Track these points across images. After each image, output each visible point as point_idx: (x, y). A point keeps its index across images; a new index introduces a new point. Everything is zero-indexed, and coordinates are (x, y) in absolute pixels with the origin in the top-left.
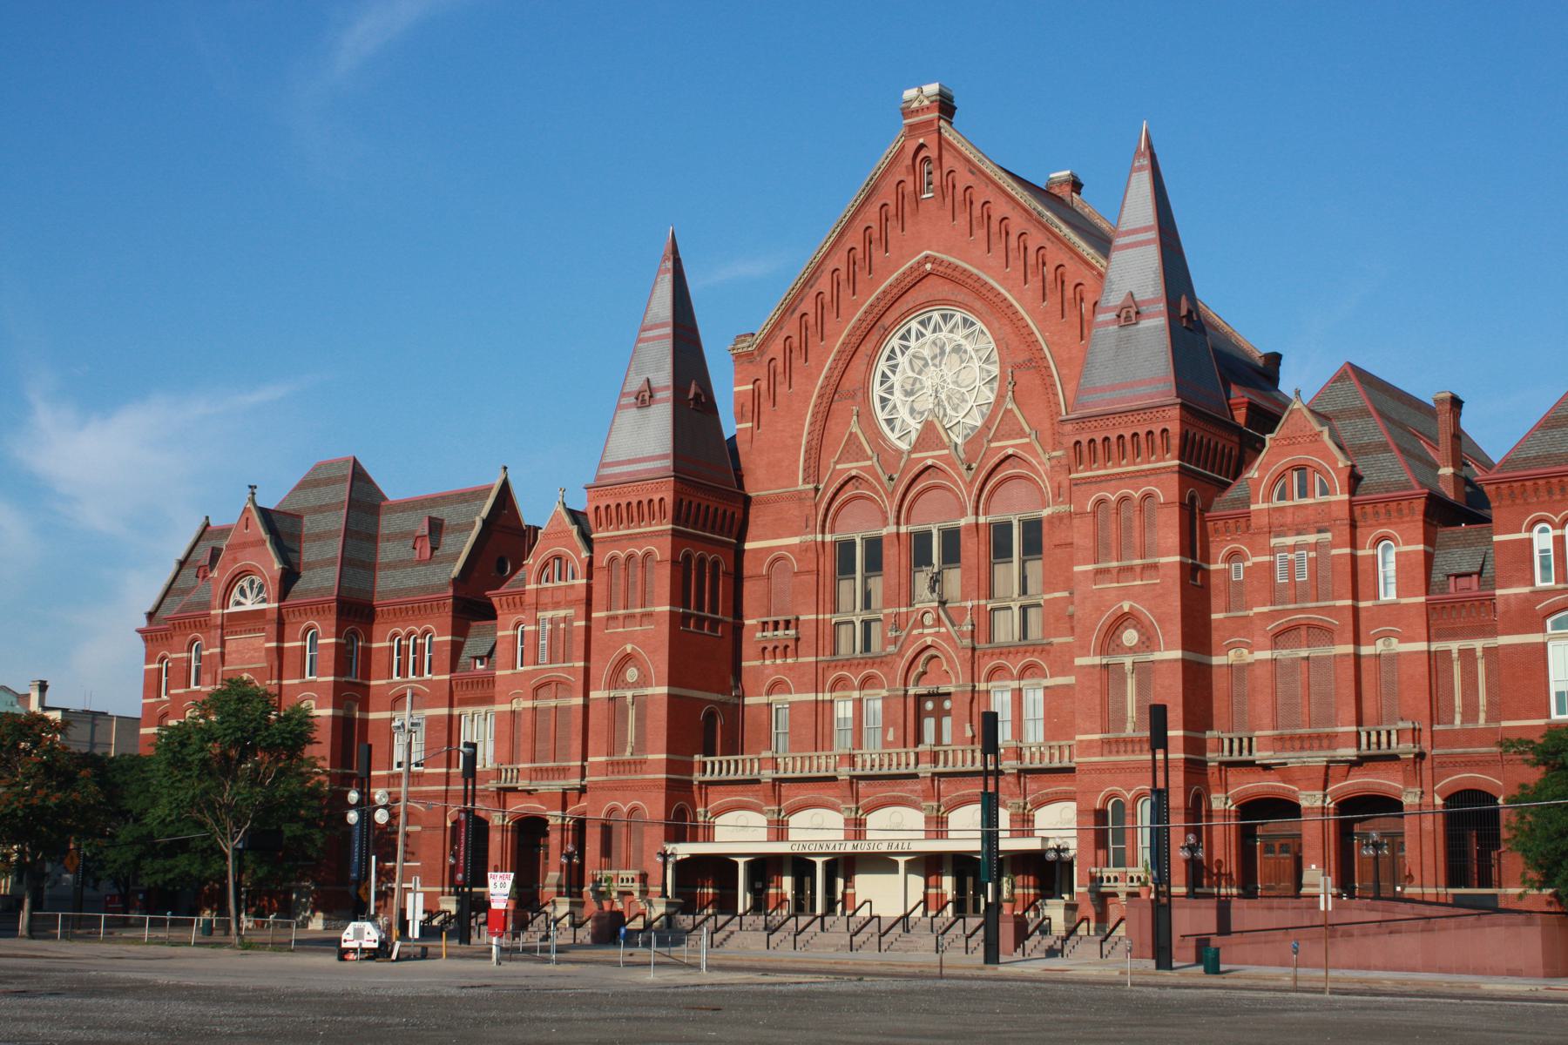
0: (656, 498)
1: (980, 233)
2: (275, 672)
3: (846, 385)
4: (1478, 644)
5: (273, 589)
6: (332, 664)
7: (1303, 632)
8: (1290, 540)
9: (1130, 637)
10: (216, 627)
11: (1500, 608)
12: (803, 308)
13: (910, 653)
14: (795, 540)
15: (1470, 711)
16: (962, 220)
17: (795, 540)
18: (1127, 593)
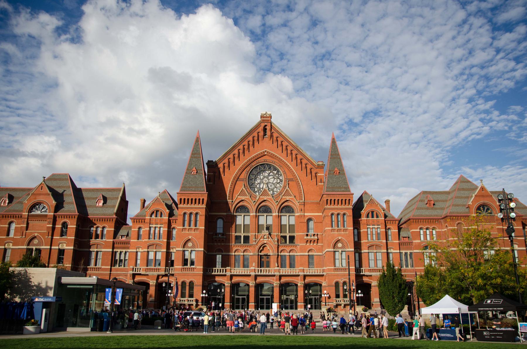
0: (201, 198)
1: (280, 148)
2: (50, 234)
3: (240, 177)
4: (409, 252)
5: (53, 209)
6: (74, 233)
7: (375, 246)
8: (371, 227)
9: (340, 245)
10: (25, 218)
11: (414, 244)
12: (229, 157)
13: (260, 244)
14: (225, 214)
15: (407, 266)
16: (275, 144)
17: (225, 214)
18: (340, 235)
